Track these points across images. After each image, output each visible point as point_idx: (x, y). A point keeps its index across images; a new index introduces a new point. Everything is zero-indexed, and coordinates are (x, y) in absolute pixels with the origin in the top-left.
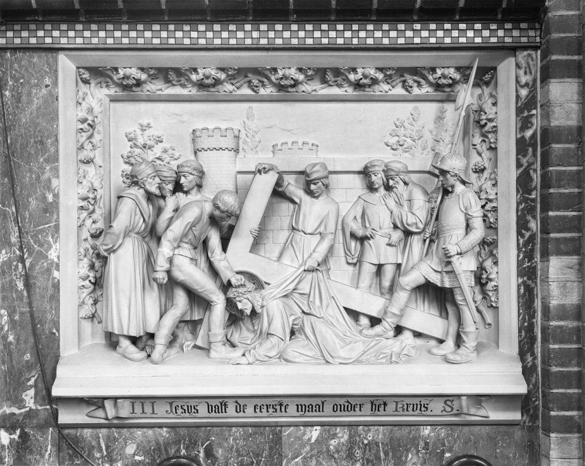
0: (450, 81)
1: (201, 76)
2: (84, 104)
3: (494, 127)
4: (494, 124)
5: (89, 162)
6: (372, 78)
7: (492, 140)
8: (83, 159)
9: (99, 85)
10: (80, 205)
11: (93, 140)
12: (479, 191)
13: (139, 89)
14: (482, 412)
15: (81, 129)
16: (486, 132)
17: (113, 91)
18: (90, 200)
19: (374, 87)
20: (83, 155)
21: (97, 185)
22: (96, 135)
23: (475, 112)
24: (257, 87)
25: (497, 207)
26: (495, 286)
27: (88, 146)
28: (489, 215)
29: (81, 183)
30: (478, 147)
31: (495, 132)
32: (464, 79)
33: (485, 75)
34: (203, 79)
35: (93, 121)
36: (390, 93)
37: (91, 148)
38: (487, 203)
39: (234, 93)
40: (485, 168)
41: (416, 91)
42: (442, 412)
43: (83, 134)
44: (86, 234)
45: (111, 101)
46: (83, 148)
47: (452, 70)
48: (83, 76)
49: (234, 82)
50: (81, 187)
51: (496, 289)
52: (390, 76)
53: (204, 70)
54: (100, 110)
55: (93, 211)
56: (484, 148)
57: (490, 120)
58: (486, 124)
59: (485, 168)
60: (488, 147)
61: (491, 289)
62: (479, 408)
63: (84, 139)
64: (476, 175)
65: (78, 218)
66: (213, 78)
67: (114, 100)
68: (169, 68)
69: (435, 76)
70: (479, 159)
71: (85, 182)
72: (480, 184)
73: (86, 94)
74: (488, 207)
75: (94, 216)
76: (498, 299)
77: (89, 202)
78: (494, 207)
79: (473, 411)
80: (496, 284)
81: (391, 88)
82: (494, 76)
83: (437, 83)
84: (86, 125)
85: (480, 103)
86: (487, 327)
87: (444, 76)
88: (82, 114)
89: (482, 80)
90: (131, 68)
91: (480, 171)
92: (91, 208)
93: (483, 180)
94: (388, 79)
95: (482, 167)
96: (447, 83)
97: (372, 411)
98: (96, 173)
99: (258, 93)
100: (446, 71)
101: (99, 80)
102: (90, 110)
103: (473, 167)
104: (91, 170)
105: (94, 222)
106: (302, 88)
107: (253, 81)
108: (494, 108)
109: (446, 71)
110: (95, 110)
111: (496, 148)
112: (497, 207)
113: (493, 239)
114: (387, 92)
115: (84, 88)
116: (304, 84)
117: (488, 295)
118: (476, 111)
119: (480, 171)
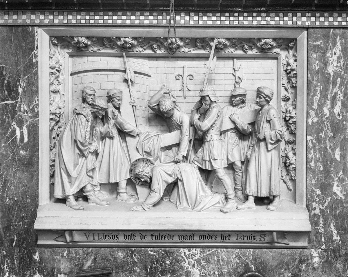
0: (270, 46)
1: (122, 42)
2: (54, 57)
3: (296, 74)
4: (294, 72)
5: (56, 92)
6: (223, 44)
7: (294, 82)
8: (53, 90)
9: (63, 47)
10: (51, 117)
11: (59, 79)
12: (285, 112)
13: (86, 49)
14: (286, 241)
15: (52, 73)
16: (290, 77)
17: (70, 51)
18: (57, 114)
19: (224, 49)
20: (53, 88)
21: (61, 105)
22: (60, 75)
23: (284, 65)
24: (156, 49)
25: (296, 122)
26: (294, 167)
27: (56, 83)
28: (291, 126)
29: (52, 104)
30: (286, 85)
31: (296, 77)
32: (278, 45)
33: (290, 43)
34: (124, 44)
35: (59, 68)
36: (234, 53)
37: (58, 83)
38: (290, 119)
39: (142, 52)
40: (289, 98)
41: (249, 52)
42: (259, 241)
43: (53, 75)
44: (54, 135)
45: (70, 56)
46: (53, 84)
47: (271, 40)
48: (53, 42)
49: (143, 45)
50: (52, 106)
51: (295, 169)
52: (234, 43)
53: (124, 39)
54: (63, 61)
55: (59, 121)
56: (289, 86)
57: (292, 70)
58: (290, 72)
59: (289, 98)
60: (291, 86)
61: (292, 169)
62: (283, 239)
63: (54, 78)
64: (283, 103)
65: (50, 125)
66: (130, 44)
67: (71, 56)
68: (104, 37)
69: (260, 43)
70: (286, 93)
71: (54, 104)
72: (286, 108)
73: (55, 52)
74: (291, 121)
75: (60, 124)
76: (295, 175)
77: (56, 115)
78: (294, 121)
79: (280, 241)
80: (294, 166)
81: (235, 50)
82: (296, 44)
83: (262, 47)
84: (55, 70)
85: (287, 60)
86: (289, 191)
87: (266, 43)
88: (53, 64)
89: (288, 46)
90: (81, 37)
91: (286, 100)
92: (57, 119)
93: (288, 105)
94: (234, 46)
95: (288, 98)
96: (268, 48)
97: (222, 239)
98: (61, 99)
99: (156, 52)
100: (267, 40)
101: (63, 44)
102: (57, 62)
103: (283, 98)
104: (57, 96)
105: (60, 127)
106: (182, 50)
107: (154, 45)
108: (295, 63)
109: (267, 40)
110: (60, 62)
111: (296, 87)
112: (296, 122)
113: (294, 140)
114: (232, 52)
115: (54, 49)
116: (184, 47)
117: (290, 173)
118: (285, 64)
119: (286, 100)
